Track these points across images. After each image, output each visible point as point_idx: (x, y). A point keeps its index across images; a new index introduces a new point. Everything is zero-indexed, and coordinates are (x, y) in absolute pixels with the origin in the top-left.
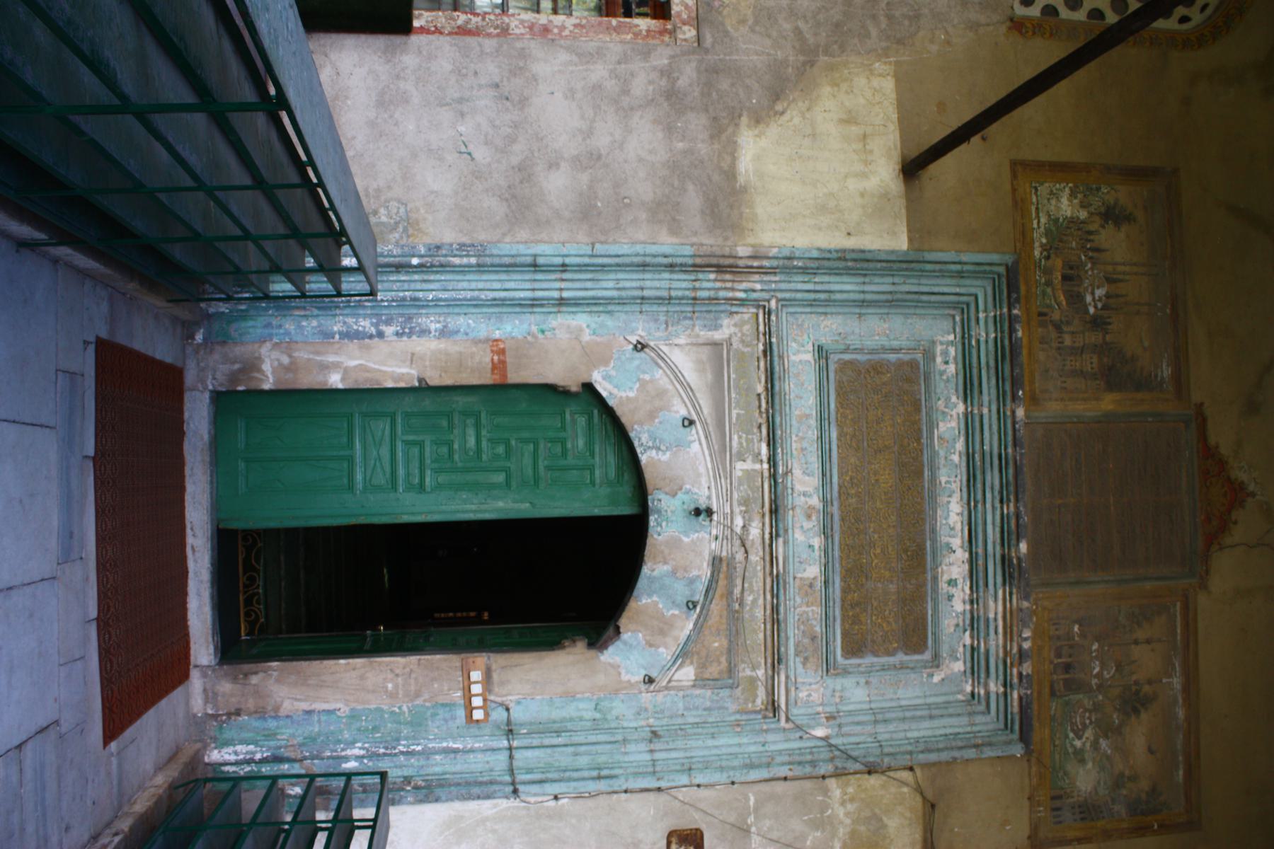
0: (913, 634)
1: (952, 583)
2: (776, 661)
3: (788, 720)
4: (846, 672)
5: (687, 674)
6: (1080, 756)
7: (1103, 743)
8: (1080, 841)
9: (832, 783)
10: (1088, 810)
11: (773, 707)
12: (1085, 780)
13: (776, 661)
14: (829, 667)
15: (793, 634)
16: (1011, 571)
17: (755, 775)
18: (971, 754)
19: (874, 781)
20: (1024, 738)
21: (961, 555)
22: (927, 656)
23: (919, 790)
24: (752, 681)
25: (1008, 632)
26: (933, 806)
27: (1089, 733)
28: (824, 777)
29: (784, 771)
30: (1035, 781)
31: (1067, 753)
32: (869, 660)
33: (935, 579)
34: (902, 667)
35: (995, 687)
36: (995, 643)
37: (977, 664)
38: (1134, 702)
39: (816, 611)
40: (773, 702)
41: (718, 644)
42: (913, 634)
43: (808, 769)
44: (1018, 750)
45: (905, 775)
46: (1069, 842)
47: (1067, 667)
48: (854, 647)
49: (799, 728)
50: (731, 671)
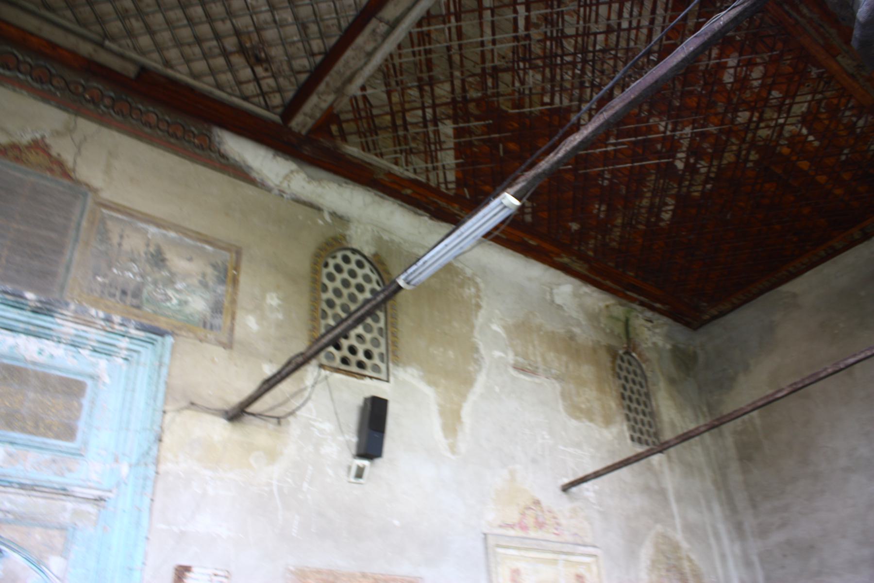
0: (72, 388)
1: (41, 352)
2: (64, 492)
3: (110, 491)
4: (86, 443)
5: (55, 563)
6: (183, 303)
7: (179, 286)
8: (233, 318)
9: (163, 468)
10: (217, 309)
11: (99, 500)
12: (198, 304)
13: (64, 492)
14: (79, 454)
15: (47, 476)
16: (45, 309)
17: (145, 522)
18: (164, 371)
19: (167, 439)
20: (161, 333)
21: (22, 341)
22: (89, 382)
23: (179, 410)
24: (75, 512)
25: (89, 323)
26: (192, 404)
27: (170, 293)
28: (157, 473)
29: (147, 500)
30: (191, 335)
31: (179, 311)
32: (81, 425)
33: (34, 363)
34: (93, 402)
35: (124, 343)
36: (94, 335)
37: (104, 350)
38: (158, 259)
39: (33, 456)
40: (96, 500)
41: (38, 535)
42: (72, 388)
43: (149, 483)
44: (169, 340)
45: (168, 417)
46: (233, 325)
47: (124, 293)
48: (68, 432)
49: (118, 485)
50: (62, 528)
